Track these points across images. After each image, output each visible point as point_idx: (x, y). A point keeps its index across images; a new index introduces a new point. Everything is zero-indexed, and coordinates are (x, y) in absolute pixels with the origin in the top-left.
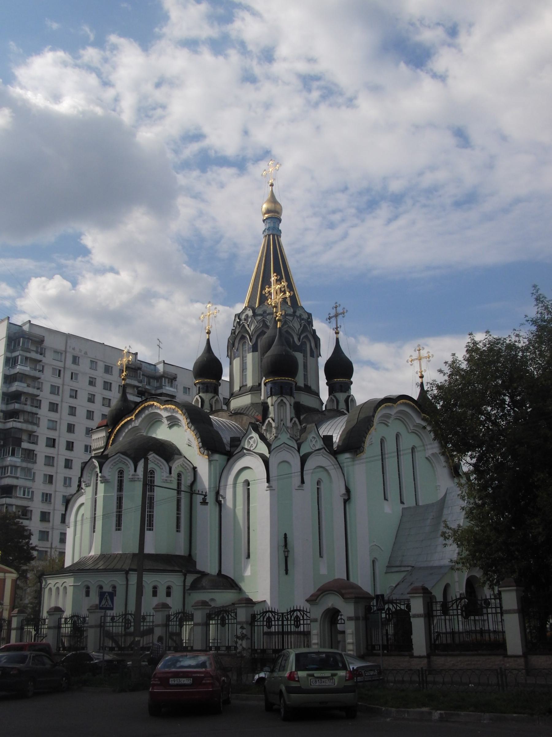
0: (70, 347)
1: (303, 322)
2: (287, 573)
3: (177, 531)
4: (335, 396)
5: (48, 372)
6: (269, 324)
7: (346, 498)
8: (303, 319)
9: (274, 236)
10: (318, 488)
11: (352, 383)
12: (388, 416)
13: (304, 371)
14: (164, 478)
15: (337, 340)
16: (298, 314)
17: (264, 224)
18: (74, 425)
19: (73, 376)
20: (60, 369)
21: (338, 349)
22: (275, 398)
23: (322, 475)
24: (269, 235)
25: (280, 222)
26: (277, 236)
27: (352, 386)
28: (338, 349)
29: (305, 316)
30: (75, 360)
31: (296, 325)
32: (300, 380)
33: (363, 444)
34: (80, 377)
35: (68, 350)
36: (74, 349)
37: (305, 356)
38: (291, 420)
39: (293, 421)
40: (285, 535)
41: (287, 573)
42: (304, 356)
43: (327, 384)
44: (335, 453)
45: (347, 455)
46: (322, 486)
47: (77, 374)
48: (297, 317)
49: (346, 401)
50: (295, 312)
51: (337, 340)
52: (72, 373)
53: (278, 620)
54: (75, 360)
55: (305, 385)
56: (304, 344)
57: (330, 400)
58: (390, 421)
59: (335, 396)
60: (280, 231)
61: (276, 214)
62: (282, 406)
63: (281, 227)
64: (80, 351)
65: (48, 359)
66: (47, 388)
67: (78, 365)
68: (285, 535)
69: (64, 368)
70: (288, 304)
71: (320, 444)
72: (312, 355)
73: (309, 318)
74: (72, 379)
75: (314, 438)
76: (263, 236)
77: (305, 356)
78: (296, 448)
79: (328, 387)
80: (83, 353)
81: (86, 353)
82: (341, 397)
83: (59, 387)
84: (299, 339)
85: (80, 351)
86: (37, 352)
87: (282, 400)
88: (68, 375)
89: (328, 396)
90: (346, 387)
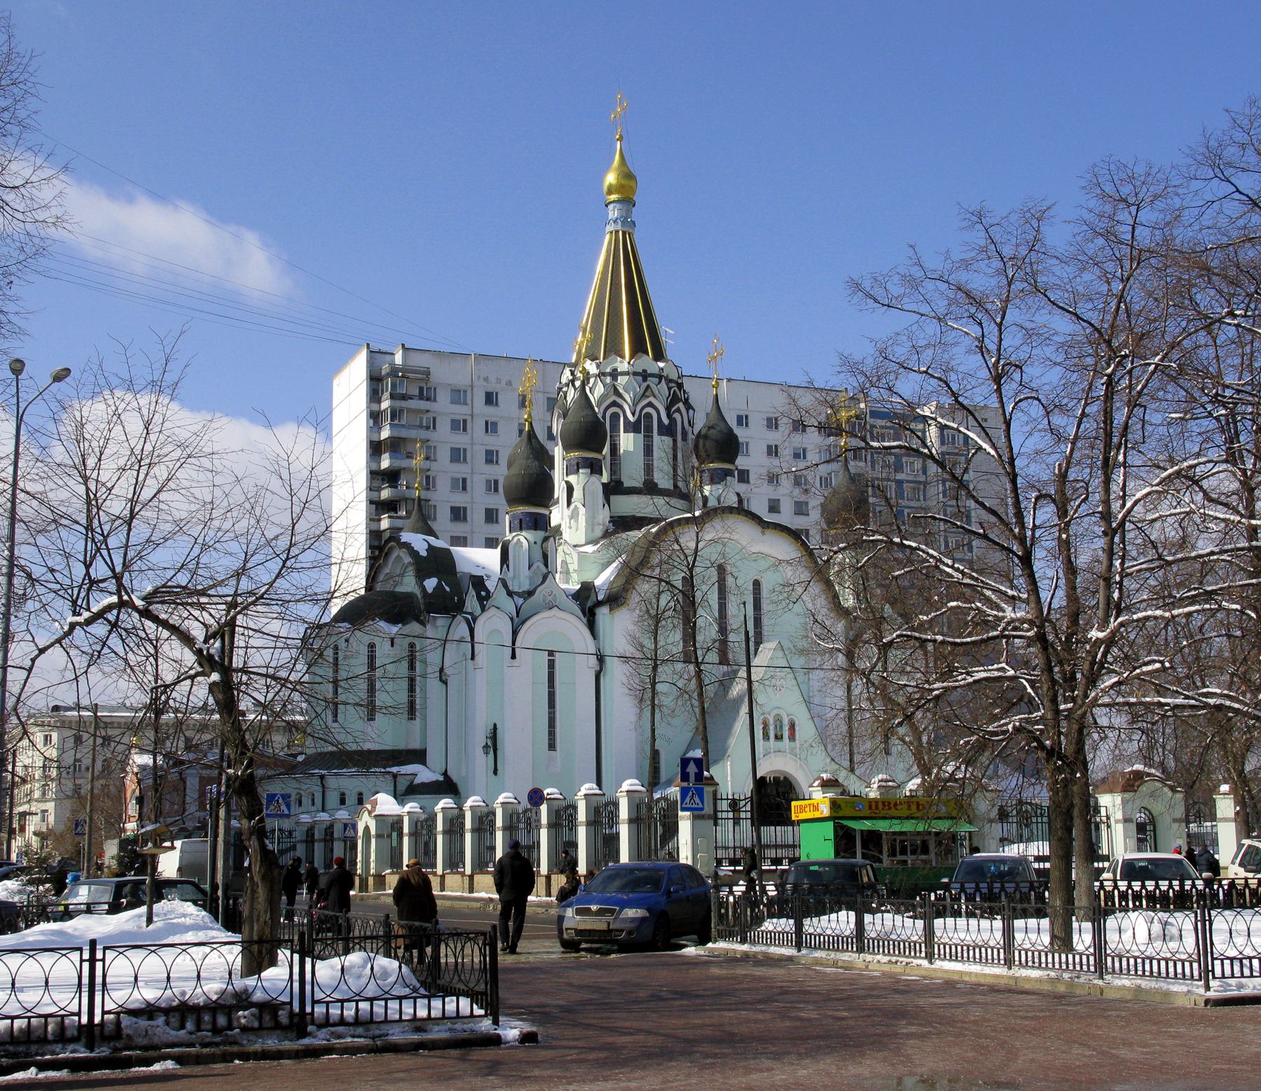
0: (479, 377)
2: (495, 772)
3: (412, 719)
5: (444, 426)
14: (386, 652)
18: (497, 510)
19: (490, 427)
20: (465, 417)
25: (634, 205)
30: (490, 399)
34: (500, 427)
35: (476, 383)
36: (486, 379)
40: (495, 725)
41: (495, 772)
47: (495, 424)
52: (487, 423)
53: (1042, 815)
54: (490, 399)
64: (499, 381)
65: (443, 406)
66: (443, 455)
67: (497, 404)
68: (495, 725)
69: (472, 416)
74: (487, 431)
80: (504, 382)
81: (509, 383)
83: (465, 450)
85: (499, 381)
86: (421, 397)
88: (479, 427)
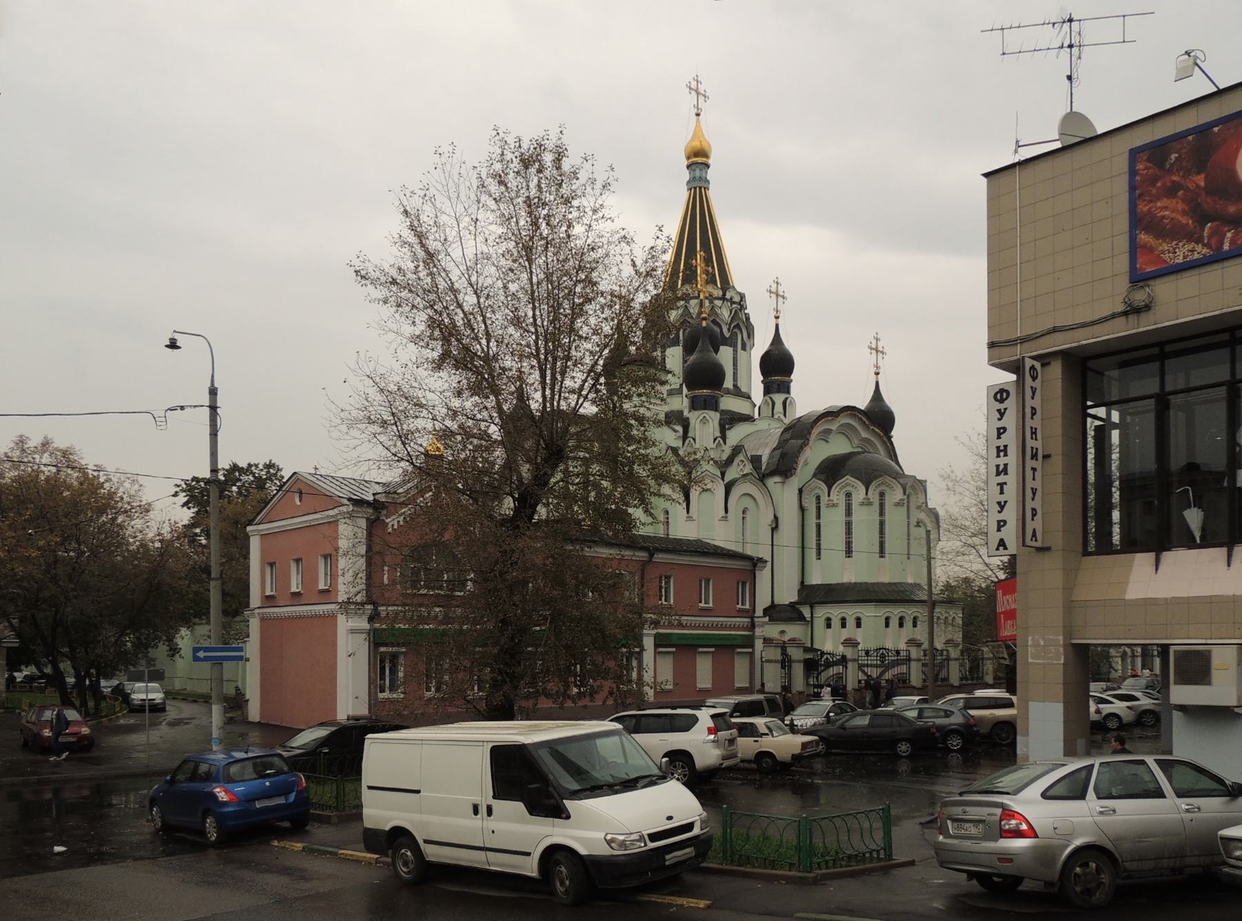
1: (734, 306)
4: (771, 398)
6: (692, 311)
7: (774, 526)
8: (734, 303)
9: (700, 188)
10: (743, 518)
11: (792, 381)
12: (828, 431)
13: (734, 369)
15: (777, 326)
16: (728, 296)
17: (688, 172)
21: (777, 339)
22: (697, 413)
23: (747, 502)
24: (695, 188)
26: (705, 188)
27: (792, 384)
28: (777, 339)
29: (737, 299)
31: (725, 313)
32: (728, 384)
33: (795, 465)
37: (735, 351)
38: (715, 440)
39: (717, 441)
42: (734, 350)
43: (762, 382)
44: (762, 478)
45: (777, 479)
46: (748, 515)
48: (727, 300)
49: (784, 403)
50: (724, 294)
51: (777, 326)
55: (734, 385)
56: (734, 335)
57: (765, 402)
58: (831, 436)
59: (771, 398)
60: (708, 182)
61: (704, 159)
62: (705, 423)
63: (711, 174)
70: (717, 286)
71: (748, 468)
72: (744, 348)
73: (741, 300)
75: (742, 461)
76: (686, 188)
77: (735, 351)
78: (720, 476)
79: (762, 386)
82: (779, 398)
84: (729, 330)
87: (705, 417)
89: (762, 398)
90: (785, 388)
